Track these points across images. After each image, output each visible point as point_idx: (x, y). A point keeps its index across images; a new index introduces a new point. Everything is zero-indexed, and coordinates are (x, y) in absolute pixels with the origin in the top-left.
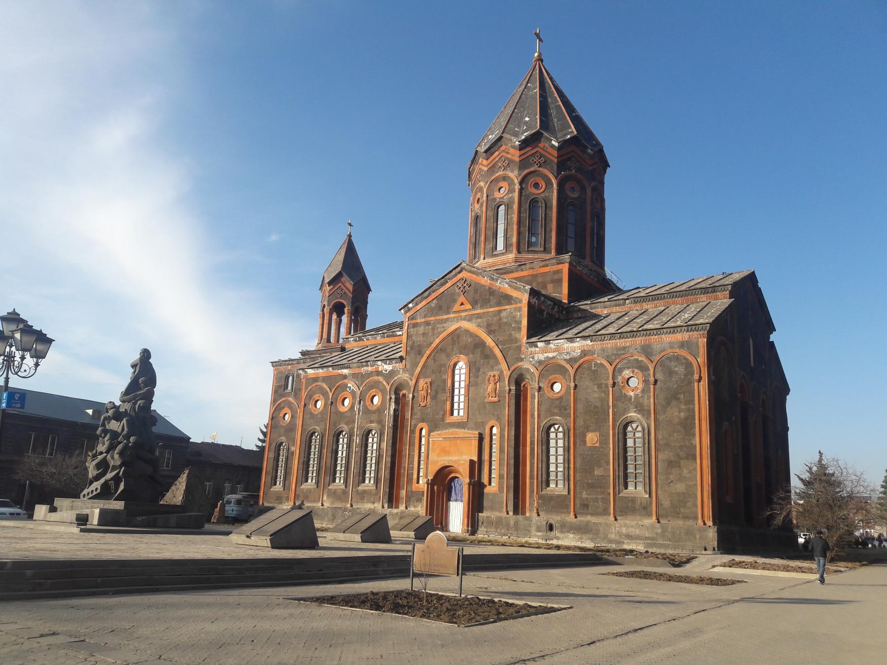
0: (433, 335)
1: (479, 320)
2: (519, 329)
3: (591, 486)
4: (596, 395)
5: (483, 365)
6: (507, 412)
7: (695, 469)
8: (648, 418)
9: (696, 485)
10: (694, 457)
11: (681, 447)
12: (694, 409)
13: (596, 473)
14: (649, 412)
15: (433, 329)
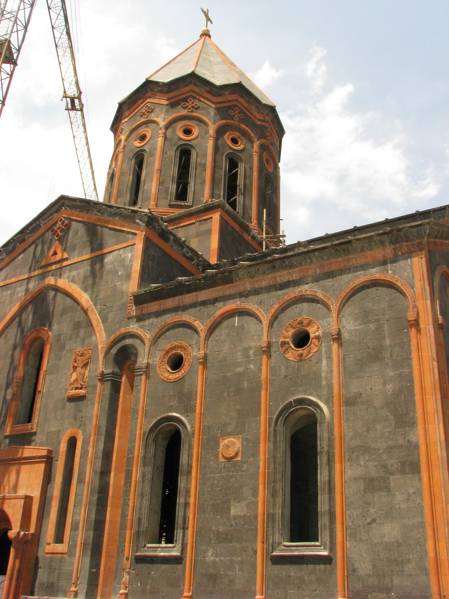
0: (11, 303)
1: (74, 273)
2: (128, 277)
3: (223, 538)
4: (240, 369)
5: (70, 339)
6: (95, 410)
7: (419, 492)
8: (328, 402)
9: (422, 525)
10: (415, 468)
11: (389, 450)
12: (411, 373)
13: (233, 511)
14: (330, 387)
15: (12, 295)
